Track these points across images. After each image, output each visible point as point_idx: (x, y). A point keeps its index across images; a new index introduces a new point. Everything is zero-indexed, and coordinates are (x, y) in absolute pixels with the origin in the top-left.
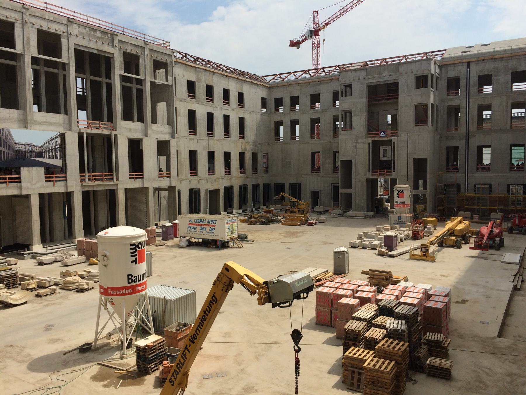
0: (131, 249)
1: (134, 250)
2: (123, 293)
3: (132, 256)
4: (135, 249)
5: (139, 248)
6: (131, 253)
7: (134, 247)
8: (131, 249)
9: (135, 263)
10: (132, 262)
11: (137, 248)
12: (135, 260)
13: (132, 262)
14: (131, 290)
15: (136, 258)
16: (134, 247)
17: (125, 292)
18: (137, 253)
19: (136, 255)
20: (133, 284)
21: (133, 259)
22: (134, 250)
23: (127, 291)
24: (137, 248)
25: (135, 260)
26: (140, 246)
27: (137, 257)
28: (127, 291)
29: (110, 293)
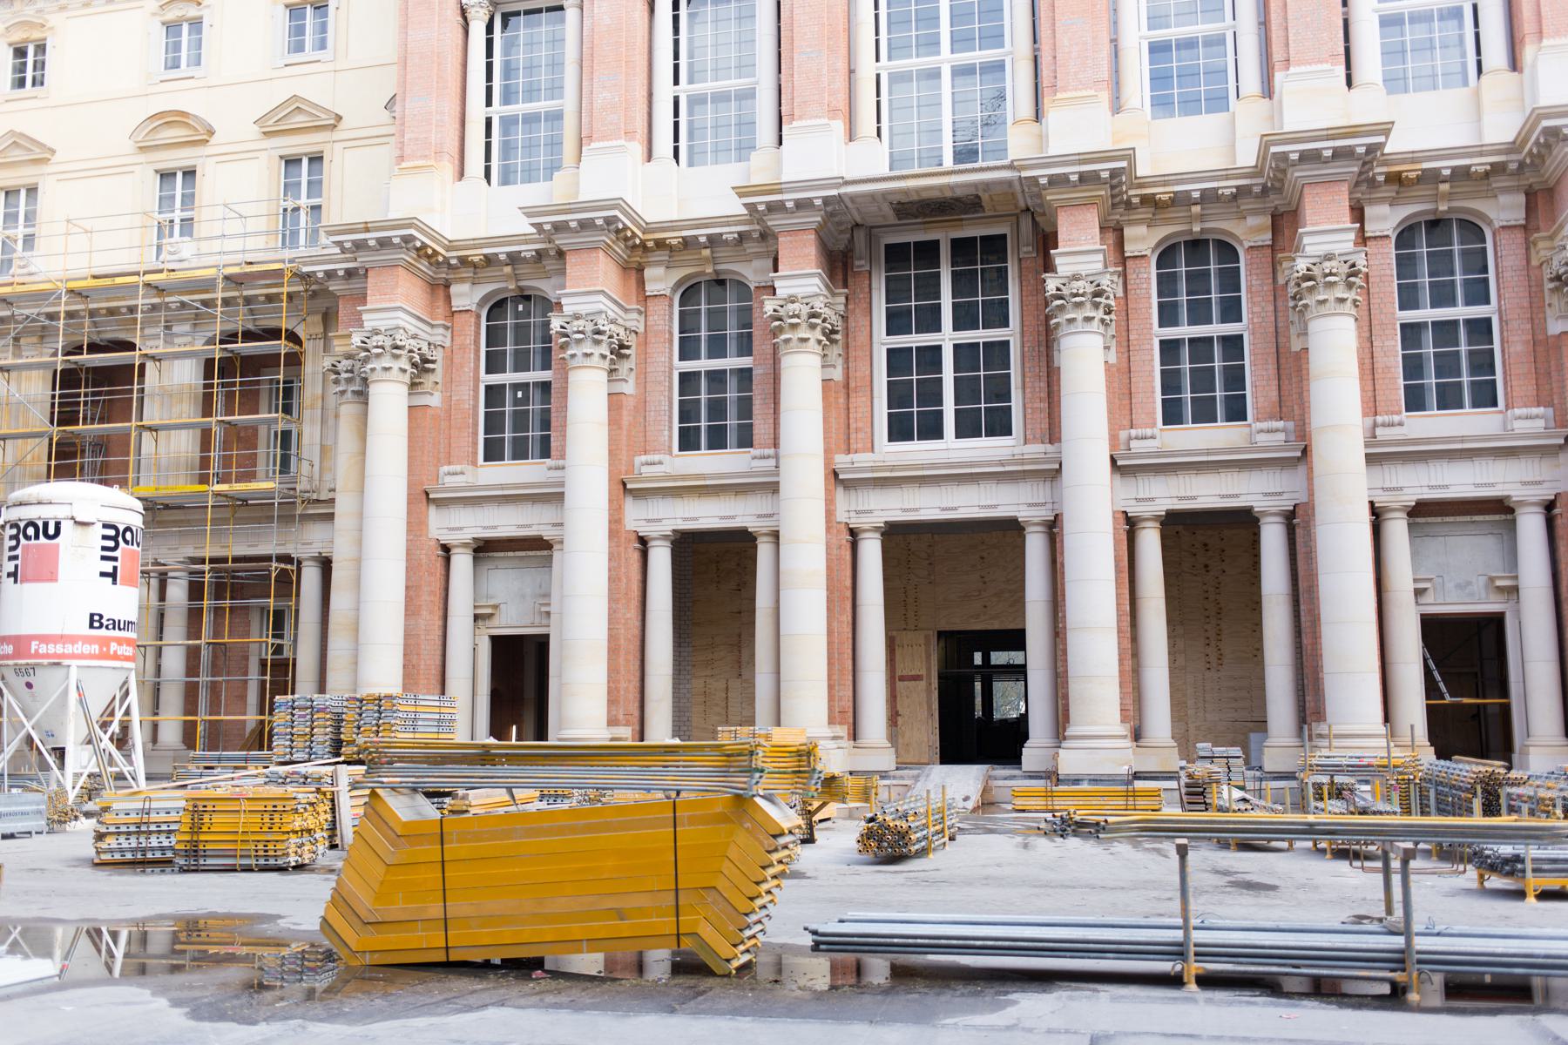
0: (105, 537)
1: (111, 544)
2: (76, 652)
3: (103, 558)
4: (115, 538)
5: (126, 542)
6: (104, 548)
7: (112, 532)
8: (105, 537)
9: (110, 579)
10: (103, 574)
11: (120, 539)
12: (111, 571)
13: (103, 574)
14: (97, 647)
15: (115, 568)
16: (112, 532)
17: (80, 652)
18: (116, 554)
19: (115, 559)
20: (103, 632)
21: (108, 567)
22: (111, 544)
23: (87, 649)
24: (120, 539)
25: (111, 571)
26: (128, 536)
27: (118, 564)
28: (87, 649)
29: (37, 651)
